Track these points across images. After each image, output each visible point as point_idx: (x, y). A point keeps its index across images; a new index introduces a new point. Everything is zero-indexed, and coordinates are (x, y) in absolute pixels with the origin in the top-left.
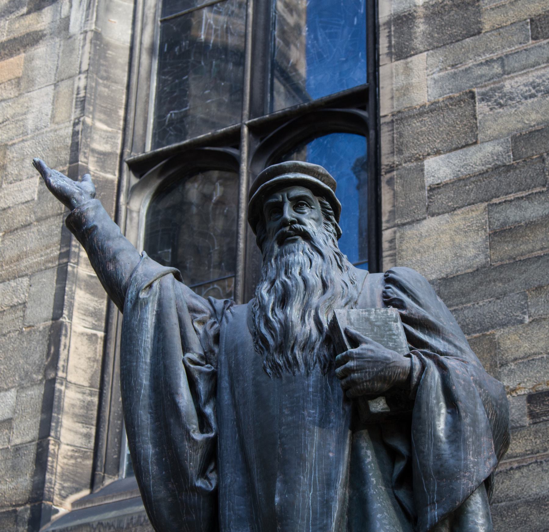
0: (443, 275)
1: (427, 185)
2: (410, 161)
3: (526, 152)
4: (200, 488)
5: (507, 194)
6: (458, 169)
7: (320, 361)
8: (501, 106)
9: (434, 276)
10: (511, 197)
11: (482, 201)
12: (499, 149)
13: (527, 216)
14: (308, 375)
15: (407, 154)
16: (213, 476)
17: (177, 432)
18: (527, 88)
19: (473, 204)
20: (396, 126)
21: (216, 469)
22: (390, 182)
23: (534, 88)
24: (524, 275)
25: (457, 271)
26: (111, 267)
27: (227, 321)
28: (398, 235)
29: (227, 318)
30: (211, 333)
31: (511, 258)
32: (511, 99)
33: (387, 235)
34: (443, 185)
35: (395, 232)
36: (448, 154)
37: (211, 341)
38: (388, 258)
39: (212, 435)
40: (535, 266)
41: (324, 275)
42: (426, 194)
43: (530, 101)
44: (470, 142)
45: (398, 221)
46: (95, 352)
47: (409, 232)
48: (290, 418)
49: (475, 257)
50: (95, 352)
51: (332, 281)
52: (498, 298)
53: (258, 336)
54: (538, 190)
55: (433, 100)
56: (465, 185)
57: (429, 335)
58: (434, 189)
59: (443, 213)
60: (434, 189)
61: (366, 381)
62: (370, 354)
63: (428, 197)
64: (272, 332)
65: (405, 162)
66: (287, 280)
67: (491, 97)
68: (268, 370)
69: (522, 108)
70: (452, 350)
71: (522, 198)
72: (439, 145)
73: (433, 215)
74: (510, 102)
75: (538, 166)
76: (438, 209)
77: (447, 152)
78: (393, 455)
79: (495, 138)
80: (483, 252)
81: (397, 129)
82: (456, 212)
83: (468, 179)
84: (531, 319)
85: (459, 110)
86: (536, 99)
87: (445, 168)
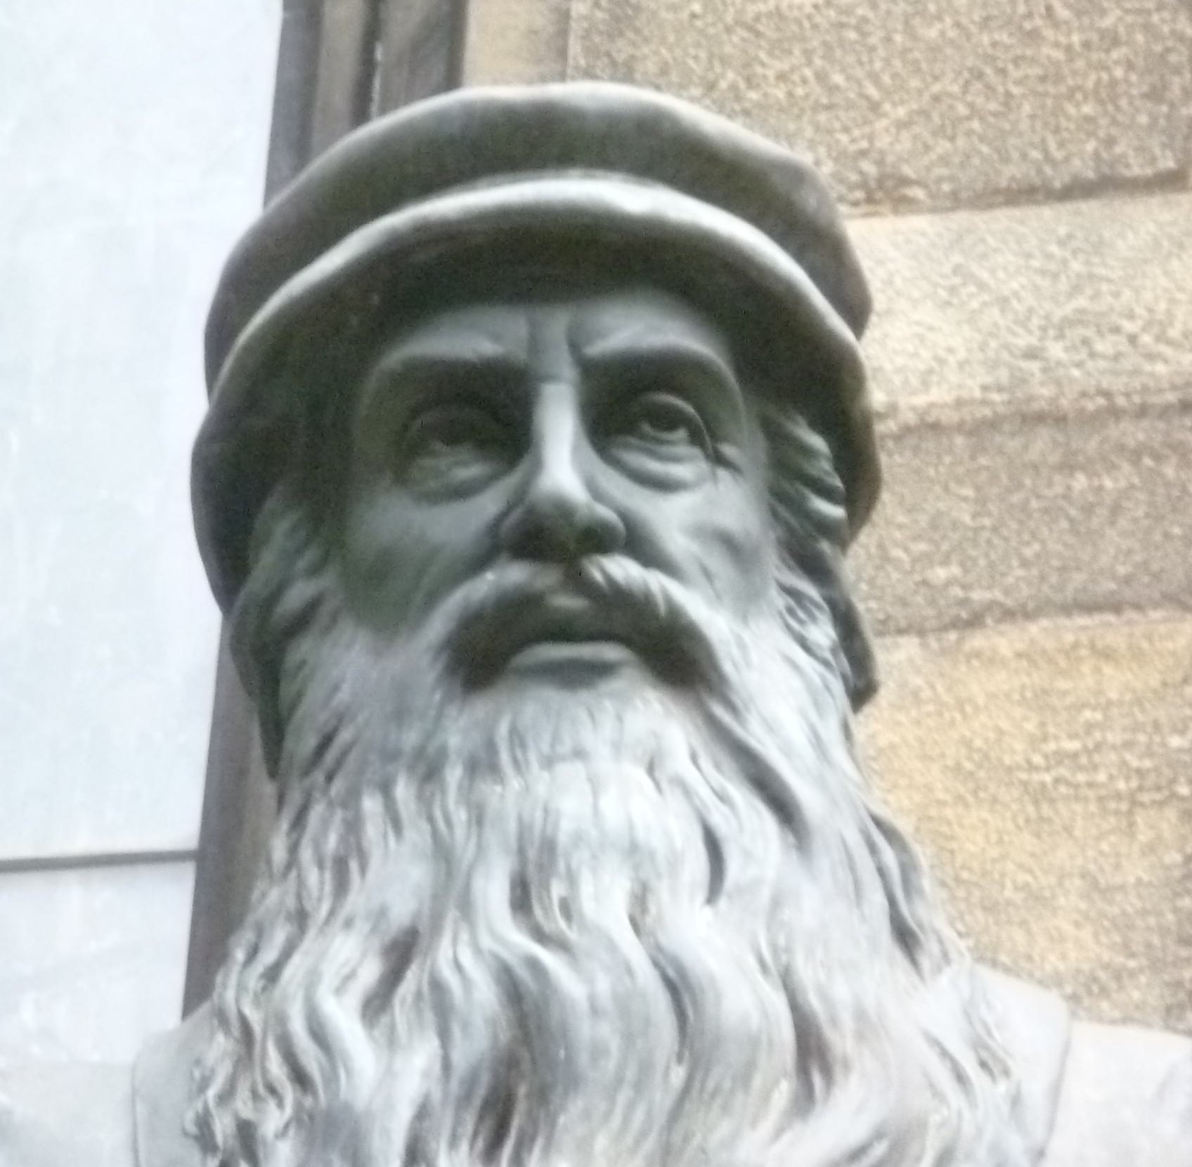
6: (1023, 340)
19: (1116, 607)
34: (907, 430)
36: (962, 218)
41: (807, 975)
44: (1137, 169)
51: (866, 1025)
56: (1068, 466)
72: (905, 143)
77: (956, 201)
80: (1156, 966)
82: (977, 641)
87: (926, 313)
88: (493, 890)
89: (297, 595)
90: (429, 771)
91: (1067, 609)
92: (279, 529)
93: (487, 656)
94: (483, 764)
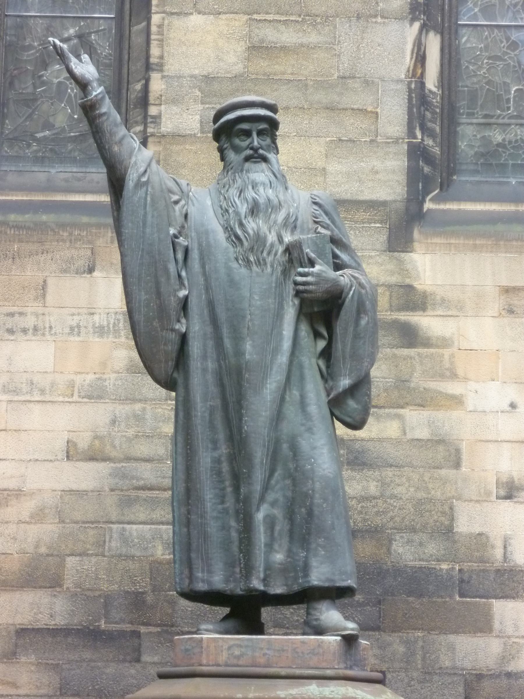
0: (205, 73)
4: (178, 330)
5: (267, 13)
7: (280, 264)
9: (197, 72)
13: (283, 39)
14: (272, 274)
16: (183, 321)
19: (237, 13)
21: (186, 316)
24: (276, 93)
25: (218, 73)
26: (116, 148)
27: (194, 205)
28: (166, 22)
29: (192, 201)
30: (184, 211)
33: (156, 19)
35: (163, 19)
37: (183, 219)
38: (156, 42)
39: (186, 293)
40: (285, 87)
45: (168, 9)
47: (177, 22)
48: (258, 303)
49: (235, 64)
53: (228, 229)
54: (293, 18)
57: (341, 251)
59: (209, 13)
61: (319, 292)
62: (324, 274)
64: (246, 235)
66: (257, 196)
68: (240, 262)
70: (354, 264)
71: (280, 21)
76: (204, 8)
78: (317, 335)
80: (242, 62)
82: (220, 16)
88: (250, 187)
89: (225, 146)
90: (242, 171)
91: (231, 13)
92: (223, 138)
93: (247, 159)
94: (248, 171)
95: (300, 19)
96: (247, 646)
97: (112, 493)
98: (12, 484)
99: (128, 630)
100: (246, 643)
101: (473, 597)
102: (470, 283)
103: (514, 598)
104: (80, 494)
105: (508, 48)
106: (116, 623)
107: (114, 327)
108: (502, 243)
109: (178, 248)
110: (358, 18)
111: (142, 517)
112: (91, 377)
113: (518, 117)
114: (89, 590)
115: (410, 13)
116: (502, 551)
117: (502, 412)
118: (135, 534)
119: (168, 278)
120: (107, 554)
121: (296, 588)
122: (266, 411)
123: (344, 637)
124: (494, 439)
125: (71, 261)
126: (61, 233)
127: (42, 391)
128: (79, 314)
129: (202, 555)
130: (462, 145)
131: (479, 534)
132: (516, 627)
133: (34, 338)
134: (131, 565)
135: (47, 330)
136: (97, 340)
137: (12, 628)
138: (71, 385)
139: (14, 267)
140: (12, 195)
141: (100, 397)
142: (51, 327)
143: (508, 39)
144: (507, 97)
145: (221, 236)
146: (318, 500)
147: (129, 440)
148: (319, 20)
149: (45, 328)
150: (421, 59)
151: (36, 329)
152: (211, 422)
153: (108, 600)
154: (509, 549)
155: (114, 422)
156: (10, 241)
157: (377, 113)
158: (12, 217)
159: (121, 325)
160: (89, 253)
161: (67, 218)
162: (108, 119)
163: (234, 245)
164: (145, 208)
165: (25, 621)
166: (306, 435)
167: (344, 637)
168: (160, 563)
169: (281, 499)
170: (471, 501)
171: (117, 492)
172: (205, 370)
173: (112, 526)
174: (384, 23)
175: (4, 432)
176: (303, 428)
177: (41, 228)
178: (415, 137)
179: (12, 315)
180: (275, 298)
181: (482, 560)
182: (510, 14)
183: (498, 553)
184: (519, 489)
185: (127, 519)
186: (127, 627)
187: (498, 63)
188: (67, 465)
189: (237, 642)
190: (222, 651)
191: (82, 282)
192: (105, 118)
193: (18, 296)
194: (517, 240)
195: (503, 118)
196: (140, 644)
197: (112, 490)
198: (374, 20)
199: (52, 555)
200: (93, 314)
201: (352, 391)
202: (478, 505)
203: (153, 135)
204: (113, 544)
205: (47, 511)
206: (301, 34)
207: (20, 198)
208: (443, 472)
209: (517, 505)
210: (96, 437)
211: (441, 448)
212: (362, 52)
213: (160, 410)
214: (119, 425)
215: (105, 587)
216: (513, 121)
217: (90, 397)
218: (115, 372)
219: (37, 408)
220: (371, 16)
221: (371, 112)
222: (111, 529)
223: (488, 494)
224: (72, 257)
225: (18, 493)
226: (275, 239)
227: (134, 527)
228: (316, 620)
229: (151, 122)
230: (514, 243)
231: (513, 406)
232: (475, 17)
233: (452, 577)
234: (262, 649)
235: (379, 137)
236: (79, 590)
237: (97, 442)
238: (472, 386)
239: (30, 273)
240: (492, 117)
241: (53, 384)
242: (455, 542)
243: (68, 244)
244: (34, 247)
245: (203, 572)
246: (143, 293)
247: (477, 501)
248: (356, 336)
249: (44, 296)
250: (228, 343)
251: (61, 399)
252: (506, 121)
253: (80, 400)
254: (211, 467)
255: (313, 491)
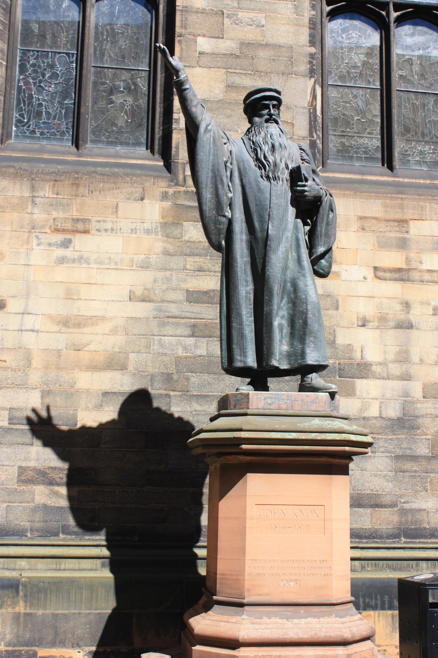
1: (198, 50)
2: (190, 35)
3: (246, 52)
5: (236, 69)
8: (236, 24)
10: (237, 71)
11: (224, 68)
12: (233, 45)
13: (244, 83)
15: (189, 31)
17: (221, 192)
18: (248, 20)
20: (184, 14)
22: (180, 41)
23: (252, 21)
25: (210, 98)
26: (194, 109)
27: (234, 146)
30: (230, 150)
31: (235, 100)
32: (241, 23)
42: (197, 55)
43: (250, 27)
46: (2, 73)
48: (275, 201)
50: (2, 73)
52: (228, 117)
54: (249, 72)
55: (203, 7)
56: (216, 58)
58: (201, 54)
59: (205, 67)
60: (201, 54)
63: (199, 57)
65: (188, 35)
67: (232, 17)
69: (245, 29)
71: (242, 73)
73: (200, 67)
74: (240, 24)
75: (251, 61)
77: (208, 37)
79: (232, 39)
81: (185, 15)
82: (211, 69)
83: (218, 55)
84: (242, 132)
85: (216, 18)
86: (252, 27)
88: (269, 136)
93: (267, 121)
95: (253, 73)
96: (275, 398)
97: (155, 319)
98: (99, 313)
99: (164, 393)
100: (274, 396)
101: (346, 378)
102: (342, 214)
103: (366, 378)
104: (136, 319)
105: (353, 98)
106: (157, 390)
107: (155, 230)
108: (358, 193)
109: (227, 169)
110: (283, 74)
111: (171, 333)
112: (142, 257)
113: (358, 133)
114: (142, 371)
115: (309, 74)
116: (360, 353)
117: (360, 281)
118: (167, 342)
119: (223, 185)
120: (152, 352)
121: (296, 365)
122: (279, 264)
123: (330, 393)
124: (356, 295)
125: (131, 194)
126: (126, 178)
127: (116, 263)
128: (136, 222)
129: (240, 346)
130: (331, 146)
131: (348, 345)
132: (368, 393)
133: (111, 234)
134: (166, 359)
135: (119, 230)
136: (146, 236)
137: (100, 392)
138: (132, 261)
139: (100, 196)
140: (98, 159)
141: (147, 267)
142: (120, 229)
143: (352, 93)
144: (353, 122)
145: (252, 163)
146: (310, 315)
147: (164, 291)
148: (262, 74)
149: (117, 229)
150: (314, 97)
151: (112, 230)
152: (245, 270)
153: (152, 378)
154: (364, 352)
155: (155, 281)
156: (98, 182)
157: (293, 124)
158: (99, 169)
159: (159, 229)
160: (141, 190)
161: (129, 171)
162: (189, 92)
163: (260, 168)
164: (210, 145)
165: (107, 388)
166: (302, 278)
167: (330, 393)
168: (181, 358)
169: (286, 315)
170: (344, 327)
171: (157, 319)
172: (241, 240)
173: (154, 337)
174: (296, 78)
175: (95, 285)
176: (299, 274)
177: (115, 175)
178: (313, 137)
179: (99, 221)
180: (284, 200)
181: (350, 358)
182: (353, 81)
183: (358, 355)
184: (369, 321)
185: (162, 333)
186: (163, 392)
187: (348, 105)
188: (129, 303)
189: (269, 396)
190: (261, 401)
191: (138, 205)
192: (188, 91)
193: (102, 211)
194: (365, 192)
195: (351, 133)
196: (170, 401)
197: (154, 318)
198: (291, 76)
199: (121, 352)
200: (143, 222)
201: (322, 256)
202: (348, 329)
203: (175, 129)
204: (155, 347)
205: (119, 328)
206: (253, 81)
207: (102, 160)
208: (330, 312)
209: (368, 330)
210: (145, 289)
211: (329, 299)
212: (285, 92)
213: (180, 275)
214: (158, 283)
215: (151, 370)
216: (356, 135)
217: (142, 267)
218: (156, 254)
219: (113, 272)
220: (289, 74)
221: (291, 123)
222: (154, 339)
223: (353, 323)
224: (132, 192)
225: (103, 318)
226: (284, 165)
227: (167, 338)
228: (309, 384)
229: (175, 122)
230: (364, 194)
231: (365, 278)
232: (336, 81)
233: (335, 367)
234: (284, 399)
235: (294, 136)
236: (137, 371)
237: (146, 292)
238: (344, 267)
239: (109, 199)
240: (345, 132)
241: (122, 260)
242: (336, 349)
243: (130, 185)
244: (111, 186)
245: (241, 356)
246: (208, 194)
247: (348, 328)
248: (328, 224)
249: (117, 212)
250: (257, 224)
251: (126, 268)
252: (352, 134)
253: (137, 269)
254: (245, 296)
255: (307, 310)
